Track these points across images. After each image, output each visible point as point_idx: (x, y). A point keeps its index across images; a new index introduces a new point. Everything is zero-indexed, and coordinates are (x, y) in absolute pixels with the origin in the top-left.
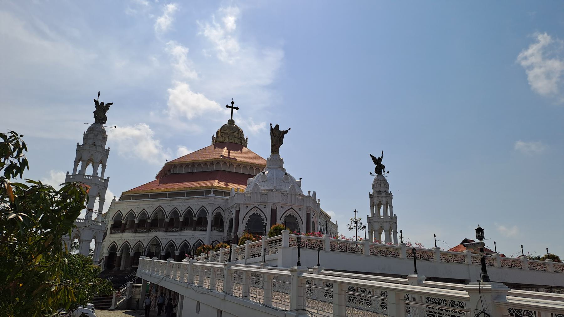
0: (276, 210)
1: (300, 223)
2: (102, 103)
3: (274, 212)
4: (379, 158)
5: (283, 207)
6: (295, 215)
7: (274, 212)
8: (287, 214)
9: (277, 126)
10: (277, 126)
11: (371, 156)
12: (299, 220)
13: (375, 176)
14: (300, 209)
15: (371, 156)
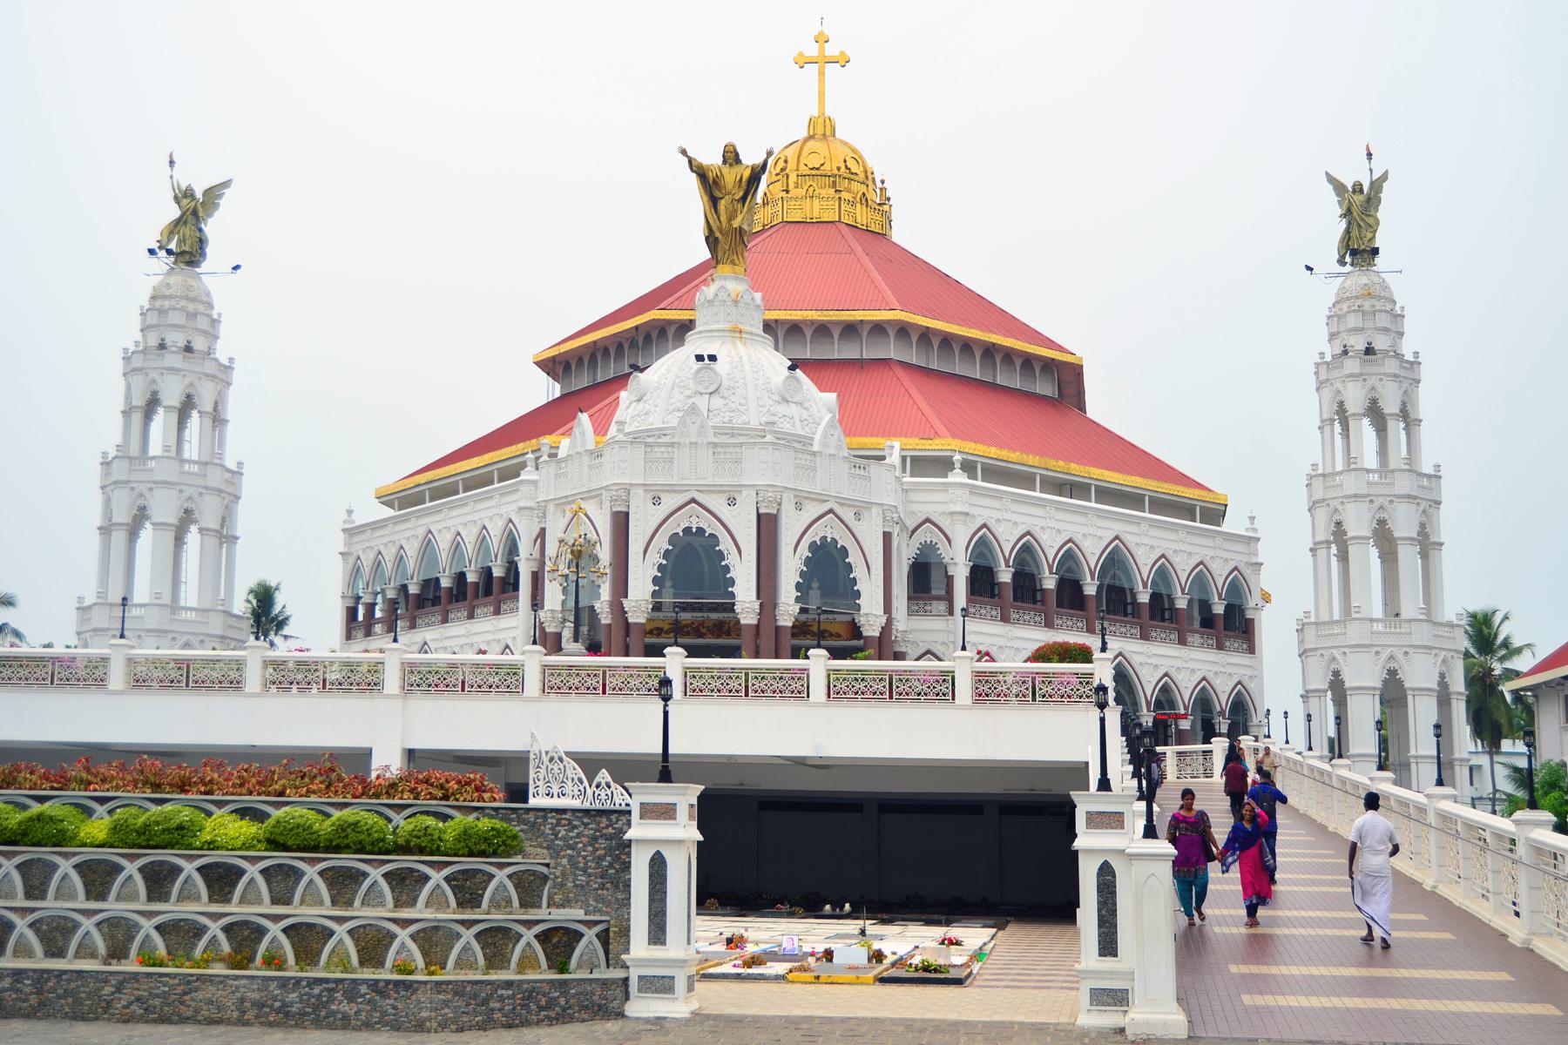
0: (627, 514)
1: (731, 559)
2: (188, 194)
3: (621, 523)
4: (1358, 188)
5: (656, 501)
6: (710, 526)
7: (621, 523)
8: (677, 525)
9: (732, 156)
10: (732, 156)
11: (1331, 179)
12: (725, 545)
13: (1332, 281)
14: (732, 502)
15: (1331, 179)
